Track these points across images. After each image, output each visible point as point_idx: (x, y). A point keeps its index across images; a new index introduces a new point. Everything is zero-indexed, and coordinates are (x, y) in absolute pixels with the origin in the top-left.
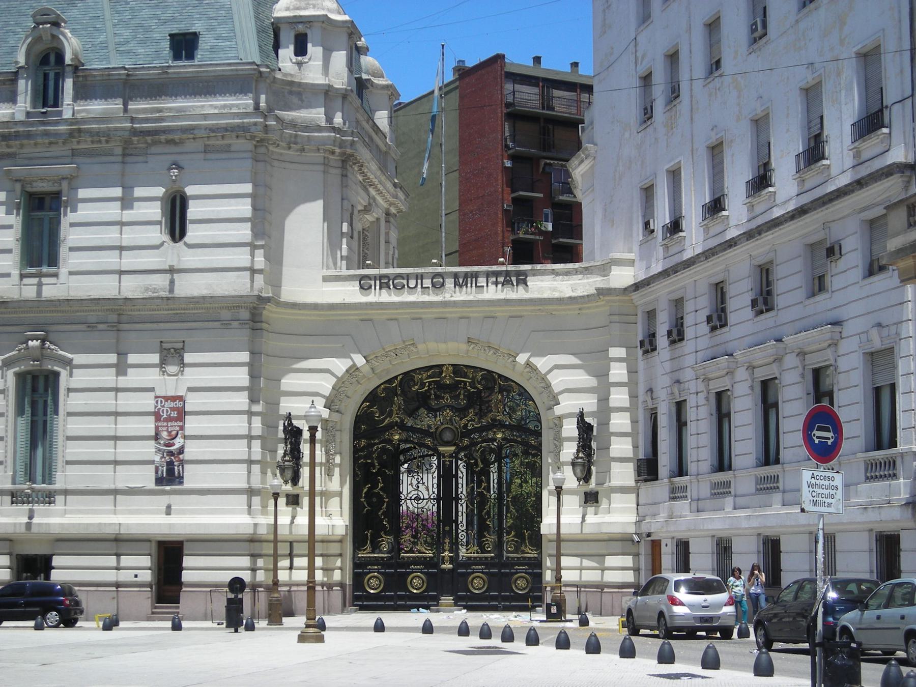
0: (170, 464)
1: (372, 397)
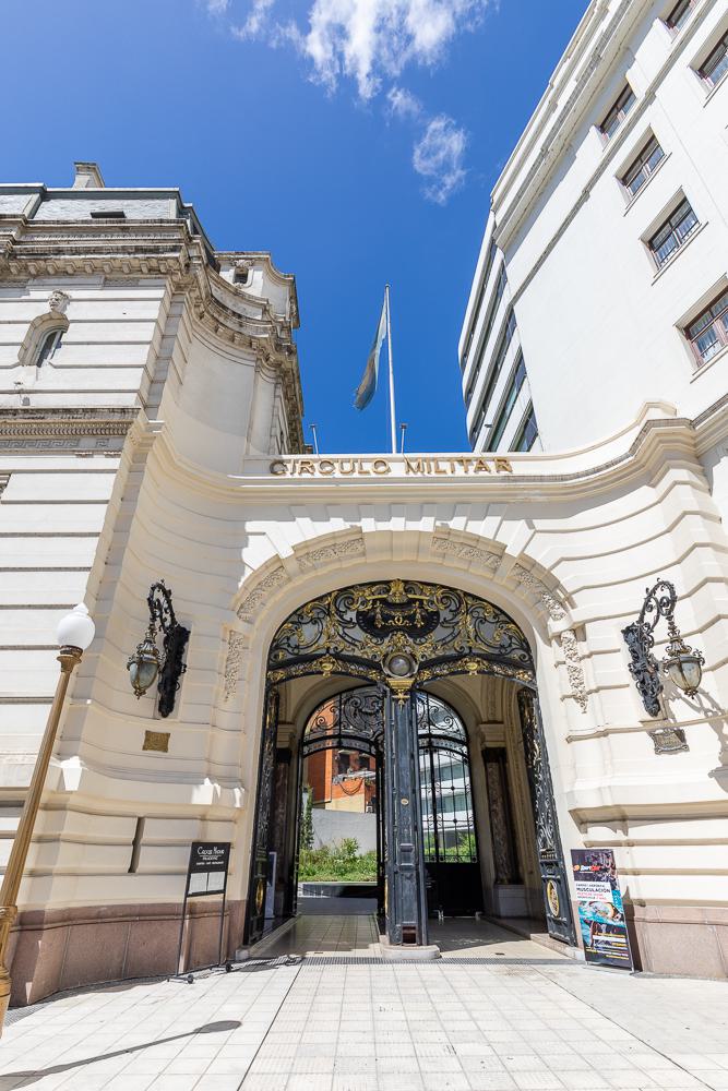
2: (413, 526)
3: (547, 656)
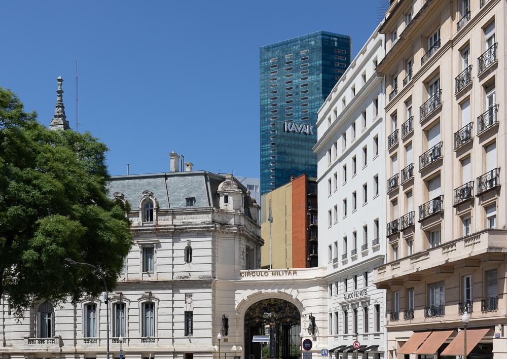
1: (250, 309)
2: (273, 291)
3: (302, 319)
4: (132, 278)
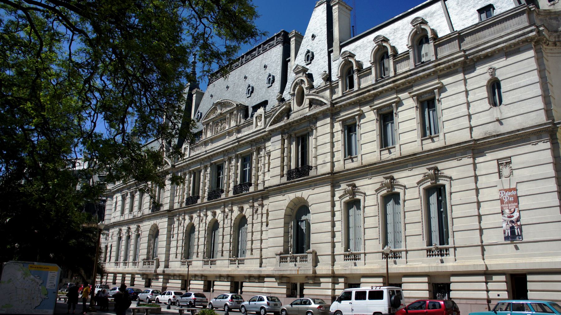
0: (512, 228)
4: (408, 150)
